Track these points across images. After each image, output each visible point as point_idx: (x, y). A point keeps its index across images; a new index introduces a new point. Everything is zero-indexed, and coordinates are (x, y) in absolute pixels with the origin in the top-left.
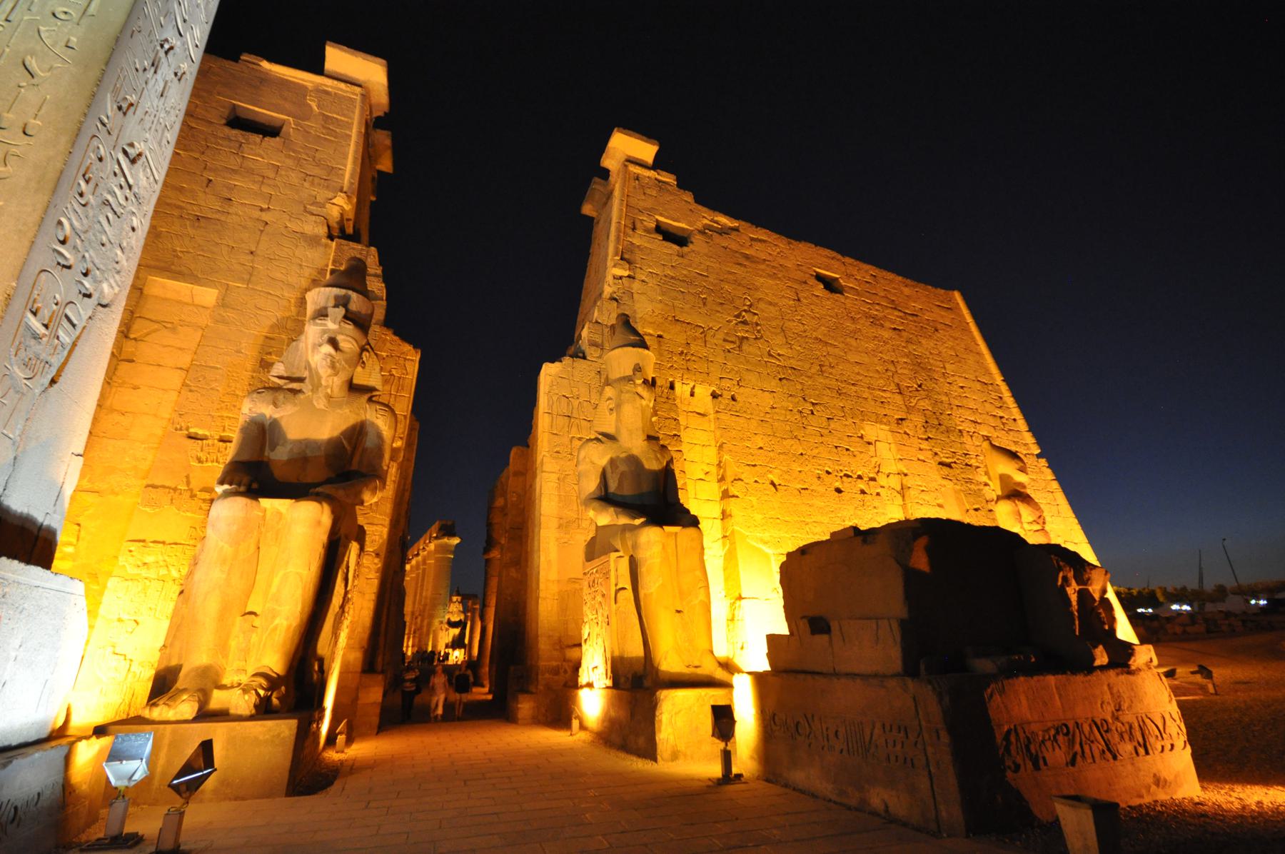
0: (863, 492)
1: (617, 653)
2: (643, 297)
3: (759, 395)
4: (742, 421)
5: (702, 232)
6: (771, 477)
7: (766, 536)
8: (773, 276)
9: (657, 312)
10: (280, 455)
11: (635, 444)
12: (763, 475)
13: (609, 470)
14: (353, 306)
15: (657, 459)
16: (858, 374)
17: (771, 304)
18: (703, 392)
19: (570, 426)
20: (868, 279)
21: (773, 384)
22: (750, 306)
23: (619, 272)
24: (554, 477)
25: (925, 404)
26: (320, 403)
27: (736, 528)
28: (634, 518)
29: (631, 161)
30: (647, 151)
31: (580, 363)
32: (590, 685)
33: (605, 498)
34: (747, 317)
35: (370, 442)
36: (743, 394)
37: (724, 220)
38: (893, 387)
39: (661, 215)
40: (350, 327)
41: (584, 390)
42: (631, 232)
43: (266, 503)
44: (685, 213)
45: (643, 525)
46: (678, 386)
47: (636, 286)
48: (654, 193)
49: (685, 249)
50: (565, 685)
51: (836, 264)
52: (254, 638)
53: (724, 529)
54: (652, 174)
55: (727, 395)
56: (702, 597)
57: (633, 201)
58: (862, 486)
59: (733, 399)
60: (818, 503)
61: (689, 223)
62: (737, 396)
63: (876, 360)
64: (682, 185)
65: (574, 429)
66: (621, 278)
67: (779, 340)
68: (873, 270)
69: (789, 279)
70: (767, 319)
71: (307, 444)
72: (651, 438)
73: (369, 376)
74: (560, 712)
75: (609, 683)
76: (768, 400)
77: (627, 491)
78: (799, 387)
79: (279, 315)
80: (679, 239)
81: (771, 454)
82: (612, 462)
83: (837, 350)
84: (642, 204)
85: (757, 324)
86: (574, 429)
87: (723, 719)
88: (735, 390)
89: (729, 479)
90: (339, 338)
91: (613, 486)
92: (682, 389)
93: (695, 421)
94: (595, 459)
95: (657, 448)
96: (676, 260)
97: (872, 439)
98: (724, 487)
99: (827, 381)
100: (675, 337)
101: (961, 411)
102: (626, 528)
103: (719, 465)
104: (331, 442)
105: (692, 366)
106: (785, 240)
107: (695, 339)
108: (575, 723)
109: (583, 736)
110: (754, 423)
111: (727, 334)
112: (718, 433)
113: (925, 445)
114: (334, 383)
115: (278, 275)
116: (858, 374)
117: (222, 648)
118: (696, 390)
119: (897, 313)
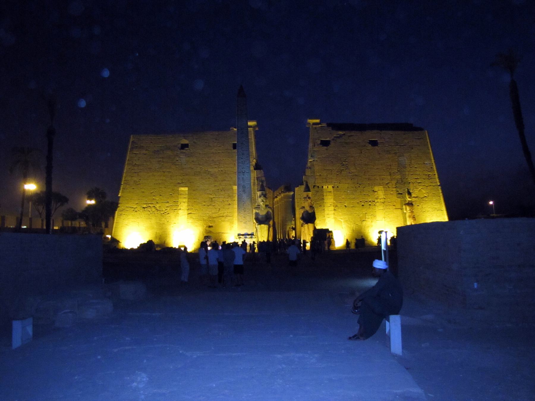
7: (342, 217)
10: (260, 217)
11: (307, 208)
17: (352, 157)
18: (330, 187)
25: (399, 177)
29: (314, 124)
37: (341, 133)
38: (388, 174)
46: (324, 187)
47: (315, 163)
55: (336, 186)
73: (268, 203)
76: (347, 185)
82: (304, 212)
93: (328, 194)
113: (394, 189)
114: (264, 206)
119: (397, 147)
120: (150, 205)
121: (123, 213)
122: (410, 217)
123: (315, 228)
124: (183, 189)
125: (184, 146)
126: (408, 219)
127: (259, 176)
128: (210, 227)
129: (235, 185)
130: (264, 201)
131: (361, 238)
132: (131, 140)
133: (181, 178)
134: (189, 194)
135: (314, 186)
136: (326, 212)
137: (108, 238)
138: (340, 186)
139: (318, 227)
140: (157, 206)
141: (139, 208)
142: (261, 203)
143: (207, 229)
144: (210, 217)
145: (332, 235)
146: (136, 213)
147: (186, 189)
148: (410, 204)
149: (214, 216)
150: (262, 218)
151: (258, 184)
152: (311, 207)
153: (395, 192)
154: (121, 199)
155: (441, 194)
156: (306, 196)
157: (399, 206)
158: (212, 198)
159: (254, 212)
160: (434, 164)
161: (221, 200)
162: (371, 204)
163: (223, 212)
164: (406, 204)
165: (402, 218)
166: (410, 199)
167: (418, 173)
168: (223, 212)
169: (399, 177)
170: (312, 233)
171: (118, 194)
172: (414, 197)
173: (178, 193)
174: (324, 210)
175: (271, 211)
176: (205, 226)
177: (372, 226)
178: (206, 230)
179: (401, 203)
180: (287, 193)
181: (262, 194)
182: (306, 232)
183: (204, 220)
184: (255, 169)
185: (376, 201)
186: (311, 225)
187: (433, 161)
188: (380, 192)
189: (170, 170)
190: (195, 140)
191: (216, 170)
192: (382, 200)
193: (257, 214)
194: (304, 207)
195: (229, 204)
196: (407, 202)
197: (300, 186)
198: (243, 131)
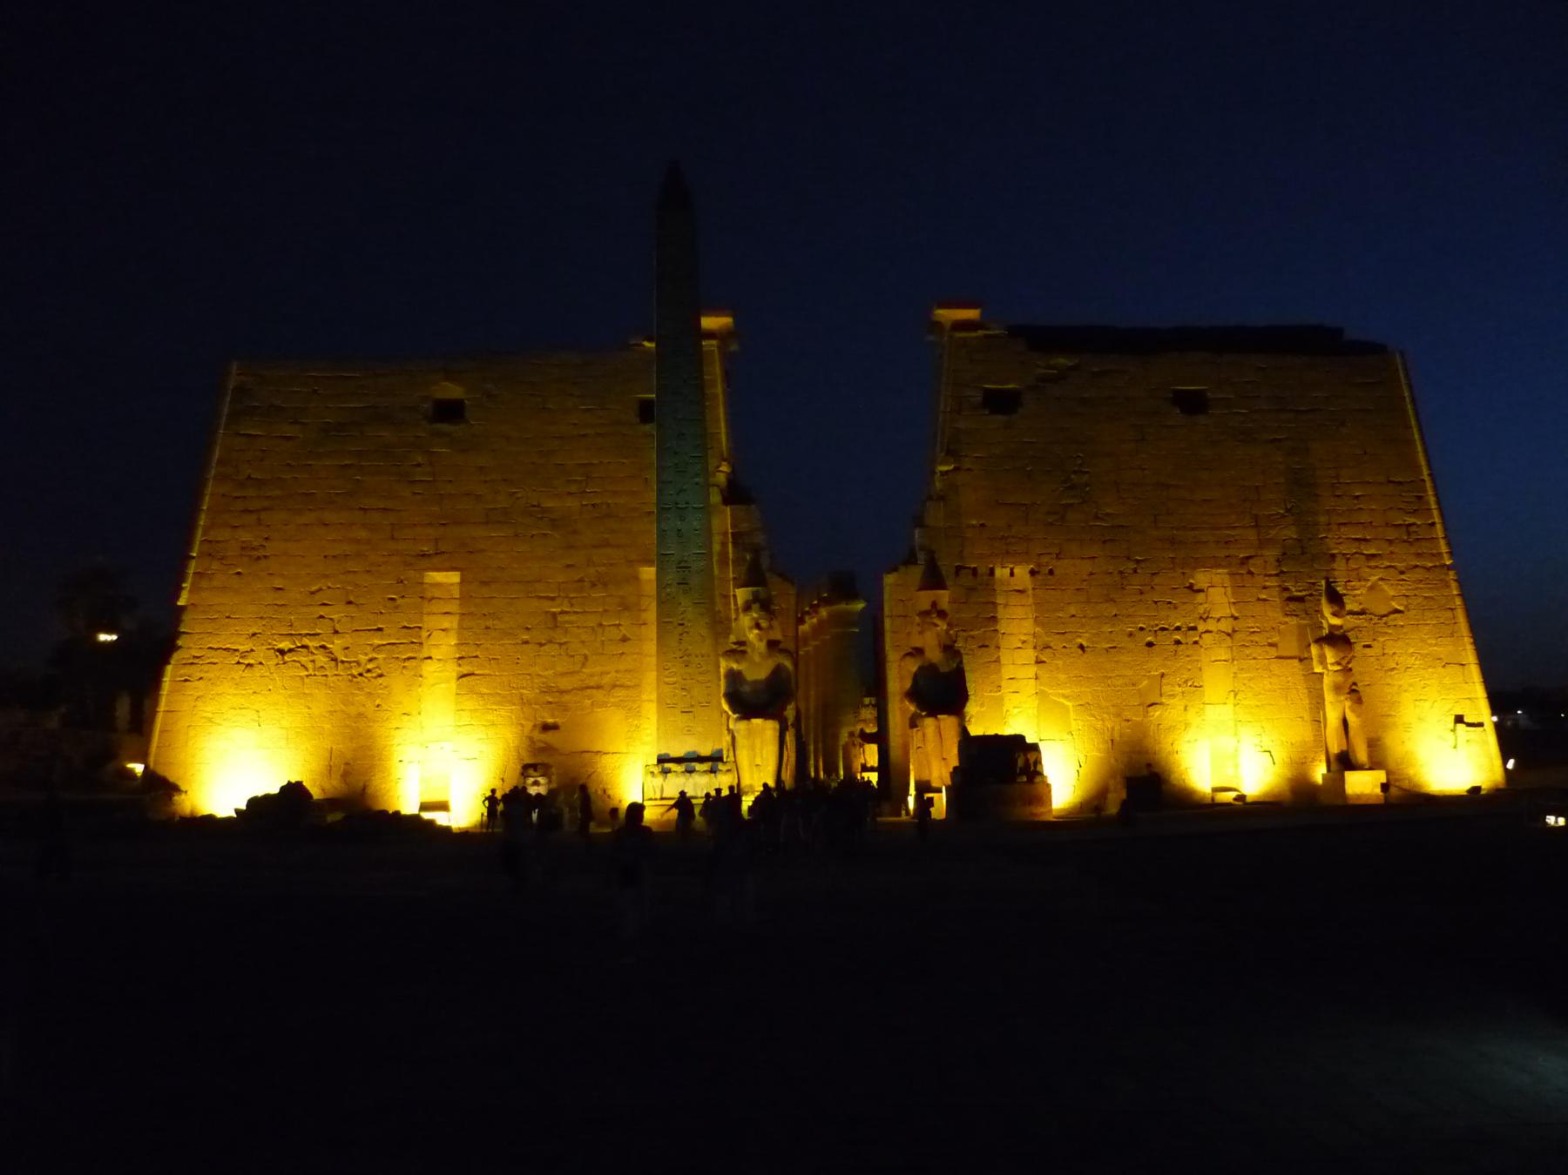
0: (1178, 642)
7: (1067, 692)
11: (934, 655)
12: (1070, 641)
18: (1022, 572)
25: (1291, 533)
26: (757, 659)
37: (1062, 361)
54: (980, 333)
59: (1051, 572)
60: (1125, 658)
62: (1057, 572)
71: (755, 682)
76: (1087, 567)
85: (1087, 485)
92: (1001, 573)
93: (1015, 599)
97: (1204, 585)
101: (1343, 529)
114: (761, 646)
118: (1016, 571)
120: (306, 641)
121: (195, 672)
122: (1337, 689)
123: (964, 731)
125: (450, 411)
126: (1329, 697)
127: (744, 526)
128: (546, 728)
129: (649, 563)
130: (764, 624)
131: (1145, 772)
132: (231, 384)
134: (465, 598)
135: (958, 569)
136: (1007, 671)
137: (131, 773)
138: (1063, 567)
139: (975, 730)
140: (336, 645)
141: (261, 653)
142: (753, 635)
143: (537, 735)
144: (547, 690)
145: (1038, 762)
146: (247, 673)
147: (453, 578)
148: (1337, 639)
149: (565, 683)
151: (736, 562)
152: (950, 649)
153: (1275, 592)
154: (186, 617)
155: (1458, 601)
156: (926, 606)
157: (1291, 647)
158: (554, 615)
159: (722, 671)
160: (1428, 484)
161: (592, 621)
162: (1184, 638)
163: (598, 669)
164: (1320, 641)
165: (1303, 693)
166: (1336, 621)
167: (1364, 518)
168: (598, 669)
169: (1291, 533)
170: (955, 751)
171: (178, 597)
172: (1351, 613)
173: (425, 597)
174: (998, 661)
175: (788, 664)
176: (529, 725)
177: (1187, 725)
178: (531, 739)
179: (1302, 635)
180: (842, 606)
182: (931, 745)
183: (524, 702)
184: (726, 501)
185: (1201, 628)
186: (948, 722)
187: (1425, 472)
188: (1217, 594)
191: (572, 503)
192: (1225, 626)
193: (734, 678)
194: (918, 652)
195: (625, 639)
196: (1326, 632)
197: (902, 569)
198: (683, 342)
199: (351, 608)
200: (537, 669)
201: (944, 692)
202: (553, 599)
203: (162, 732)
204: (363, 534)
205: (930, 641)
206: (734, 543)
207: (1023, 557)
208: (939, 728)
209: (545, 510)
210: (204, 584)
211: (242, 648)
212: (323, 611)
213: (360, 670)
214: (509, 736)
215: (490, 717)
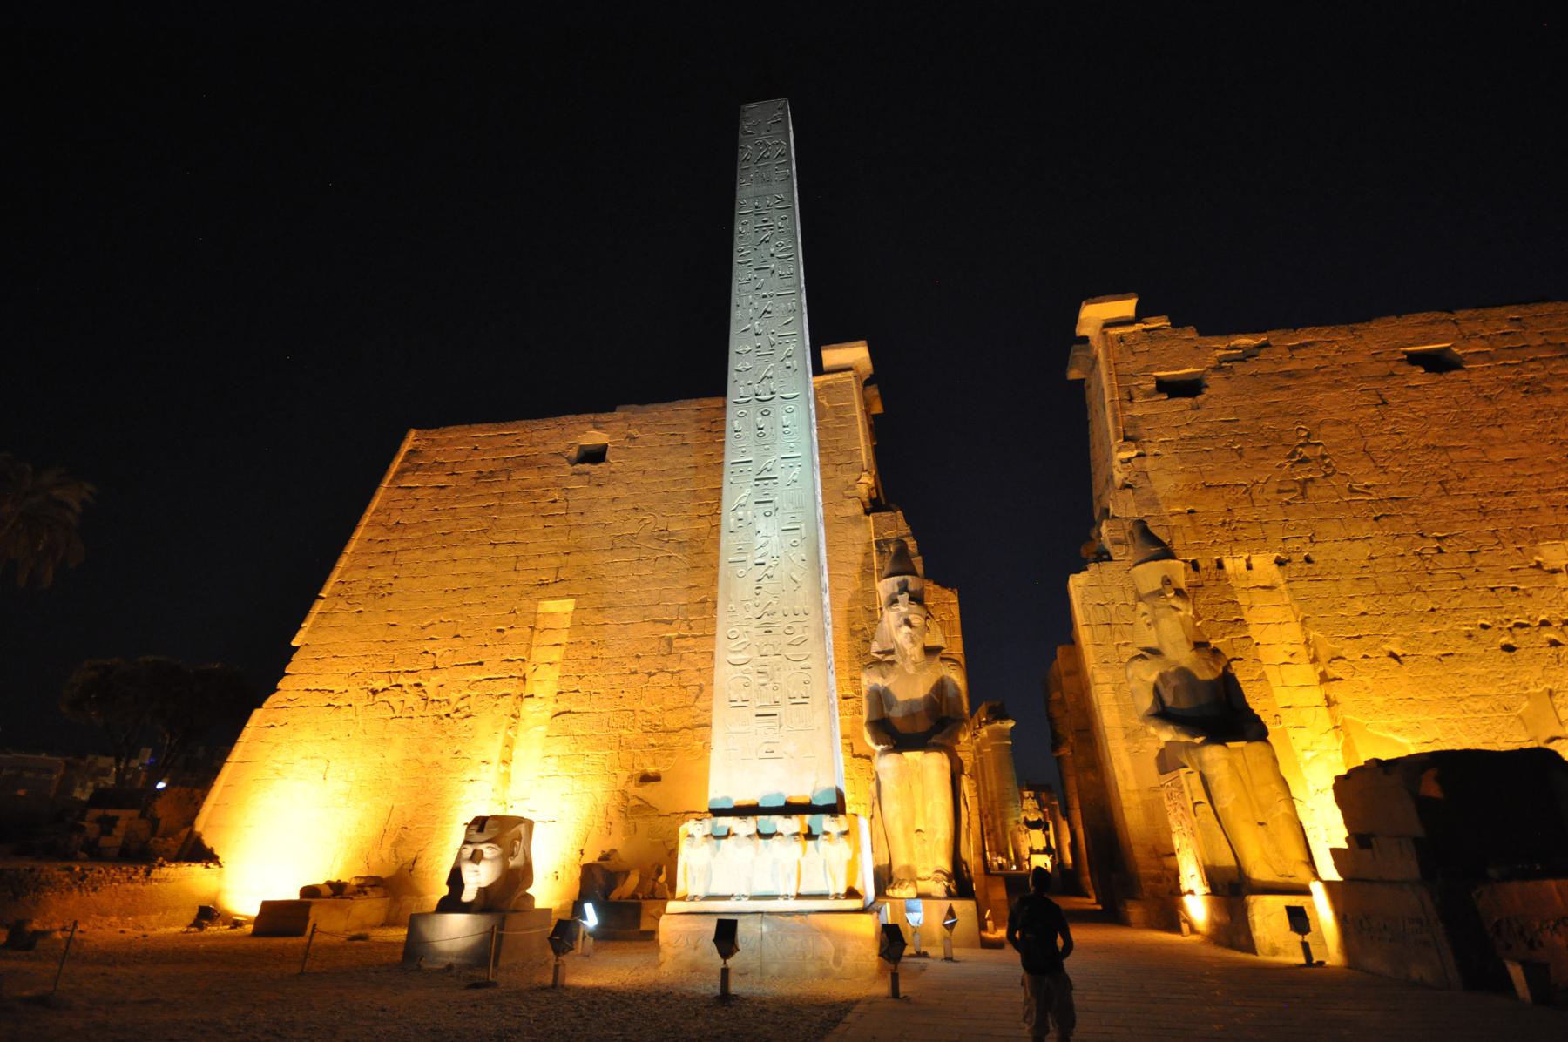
1: (1208, 863)
2: (1160, 474)
3: (1344, 549)
4: (1326, 585)
5: (1214, 369)
6: (1387, 647)
7: (1396, 722)
8: (1338, 384)
9: (1181, 485)
10: (896, 713)
11: (1184, 656)
12: (1374, 648)
13: (1160, 685)
14: (911, 588)
15: (1211, 668)
16: (1514, 476)
17: (1339, 423)
19: (1112, 633)
20: (1506, 327)
21: (1366, 528)
22: (1308, 437)
23: (1125, 455)
24: (1108, 687)
26: (911, 670)
27: (1348, 717)
28: (1194, 737)
29: (1109, 324)
30: (1126, 307)
31: (1107, 567)
32: (1191, 892)
33: (1163, 714)
34: (1306, 452)
35: (950, 693)
36: (1320, 553)
37: (1245, 341)
39: (1160, 370)
40: (915, 606)
41: (1117, 593)
42: (1128, 405)
43: (908, 755)
44: (1189, 354)
45: (1204, 743)
46: (1229, 564)
47: (1149, 463)
48: (1145, 348)
49: (1200, 398)
50: (1171, 892)
51: (1440, 329)
52: (927, 848)
53: (1333, 718)
54: (1138, 327)
55: (1298, 558)
56: (1284, 808)
57: (1122, 368)
58: (1553, 636)
59: (1308, 560)
60: (1474, 670)
61: (1199, 365)
62: (1312, 557)
63: (1545, 447)
64: (1177, 323)
65: (1117, 636)
66: (1129, 460)
67: (1364, 466)
68: (1512, 312)
69: (1362, 380)
70: (1336, 445)
71: (911, 703)
72: (1199, 646)
73: (936, 639)
74: (1169, 914)
75: (1208, 890)
76: (1361, 551)
77: (1184, 704)
78: (1410, 521)
79: (851, 590)
80: (1187, 388)
81: (1382, 618)
82: (1162, 676)
83: (1466, 454)
84: (1133, 368)
85: (1323, 457)
86: (1117, 636)
87: (1299, 920)
88: (1308, 550)
89: (1324, 660)
90: (911, 617)
91: (1169, 700)
93: (1260, 598)
94: (1143, 675)
95: (1207, 655)
96: (1191, 416)
98: (1320, 669)
99: (1458, 502)
100: (1211, 506)
102: (1188, 746)
103: (1306, 642)
104: (926, 698)
105: (1240, 535)
106: (1344, 329)
107: (1237, 501)
108: (1185, 927)
109: (1194, 937)
110: (1346, 587)
111: (1281, 482)
112: (1296, 606)
114: (915, 652)
115: (843, 558)
116: (1514, 476)
117: (911, 853)
118: (1254, 562)
120: (402, 680)
124: (550, 606)
125: (595, 455)
127: (890, 534)
128: (646, 778)
132: (406, 447)
133: (555, 561)
134: (577, 624)
138: (1320, 553)
143: (633, 789)
147: (568, 605)
149: (672, 721)
150: (911, 716)
158: (670, 641)
178: (623, 793)
180: (998, 724)
181: (903, 588)
183: (622, 744)
189: (520, 538)
190: (633, 431)
193: (880, 698)
194: (1155, 652)
199: (458, 642)
200: (643, 704)
201: (1216, 711)
202: (670, 623)
203: (226, 786)
204: (489, 567)
205: (1171, 632)
206: (880, 552)
207: (1263, 543)
208: (1231, 763)
209: (671, 534)
210: (325, 623)
211: (337, 689)
212: (428, 646)
213: (449, 710)
214: (599, 791)
215: (579, 765)
